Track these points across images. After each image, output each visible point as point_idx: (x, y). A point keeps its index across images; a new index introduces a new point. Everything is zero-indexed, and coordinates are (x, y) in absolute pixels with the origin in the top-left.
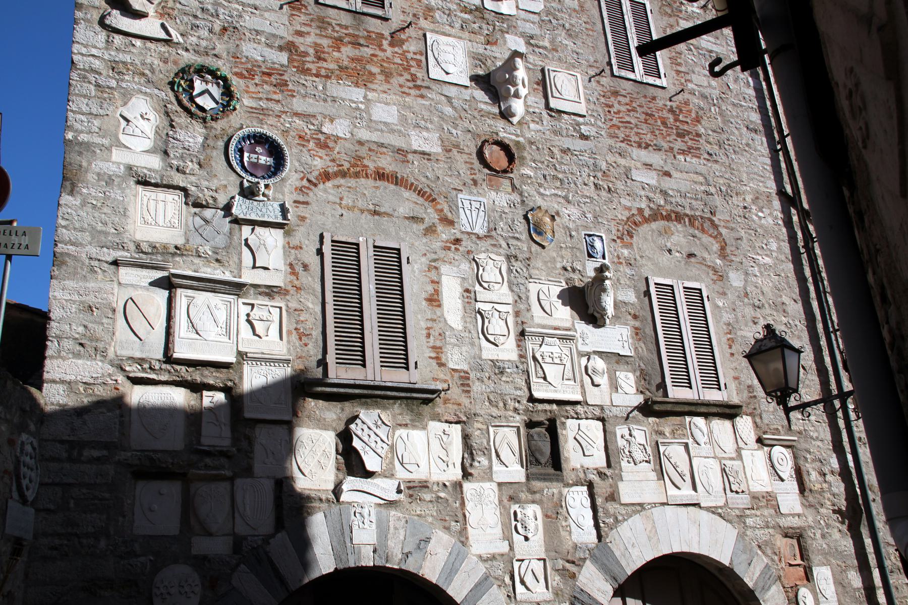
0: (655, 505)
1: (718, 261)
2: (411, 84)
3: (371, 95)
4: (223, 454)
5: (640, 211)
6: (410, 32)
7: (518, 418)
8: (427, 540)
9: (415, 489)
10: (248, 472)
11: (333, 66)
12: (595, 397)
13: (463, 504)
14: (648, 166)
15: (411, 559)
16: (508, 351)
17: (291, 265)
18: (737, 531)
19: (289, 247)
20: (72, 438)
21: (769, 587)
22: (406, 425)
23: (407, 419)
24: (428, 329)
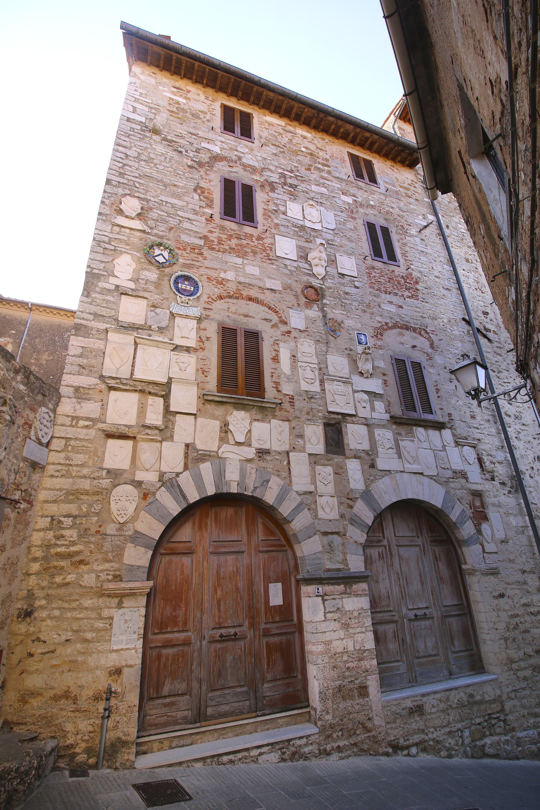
1: (430, 350)
2: (266, 258)
3: (245, 261)
4: (156, 428)
5: (387, 324)
6: (267, 234)
7: (320, 421)
8: (268, 481)
9: (262, 453)
10: (171, 438)
11: (227, 247)
12: (362, 413)
13: (289, 463)
14: (391, 303)
15: (258, 491)
16: (316, 388)
17: (200, 337)
20: (73, 415)
21: (465, 522)
22: (258, 420)
23: (259, 417)
24: (272, 373)
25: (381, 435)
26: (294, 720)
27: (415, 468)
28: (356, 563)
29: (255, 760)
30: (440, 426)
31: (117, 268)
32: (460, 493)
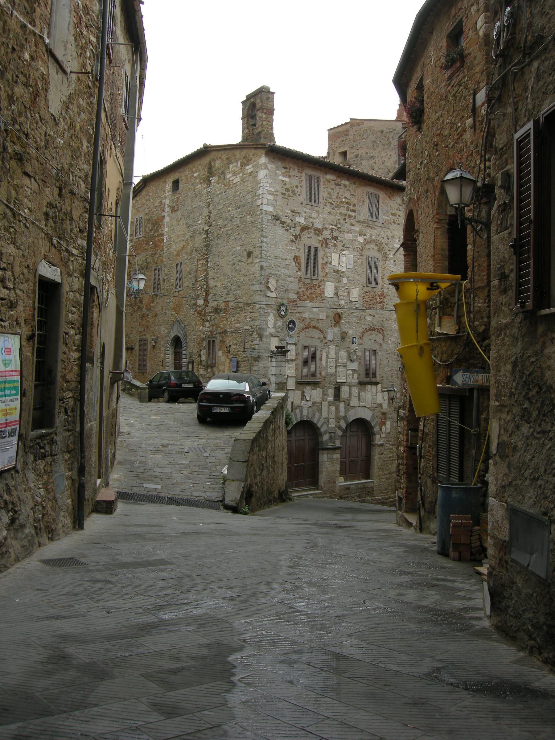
9: (314, 403)
11: (306, 297)
12: (349, 381)
16: (333, 371)
19: (297, 349)
26: (314, 489)
28: (338, 443)
29: (308, 497)
31: (269, 322)
32: (378, 414)
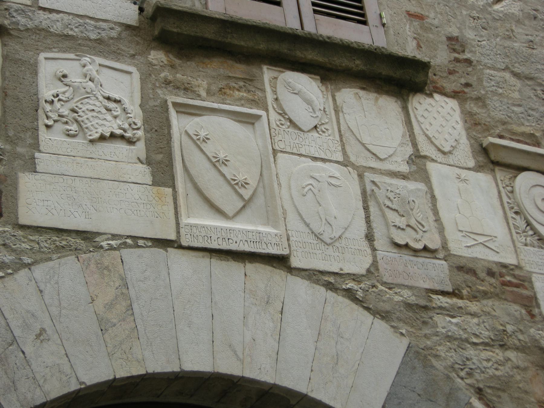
0: (135, 241)
18: (405, 342)
25: (75, 78)
27: (247, 230)
30: (398, 74)
